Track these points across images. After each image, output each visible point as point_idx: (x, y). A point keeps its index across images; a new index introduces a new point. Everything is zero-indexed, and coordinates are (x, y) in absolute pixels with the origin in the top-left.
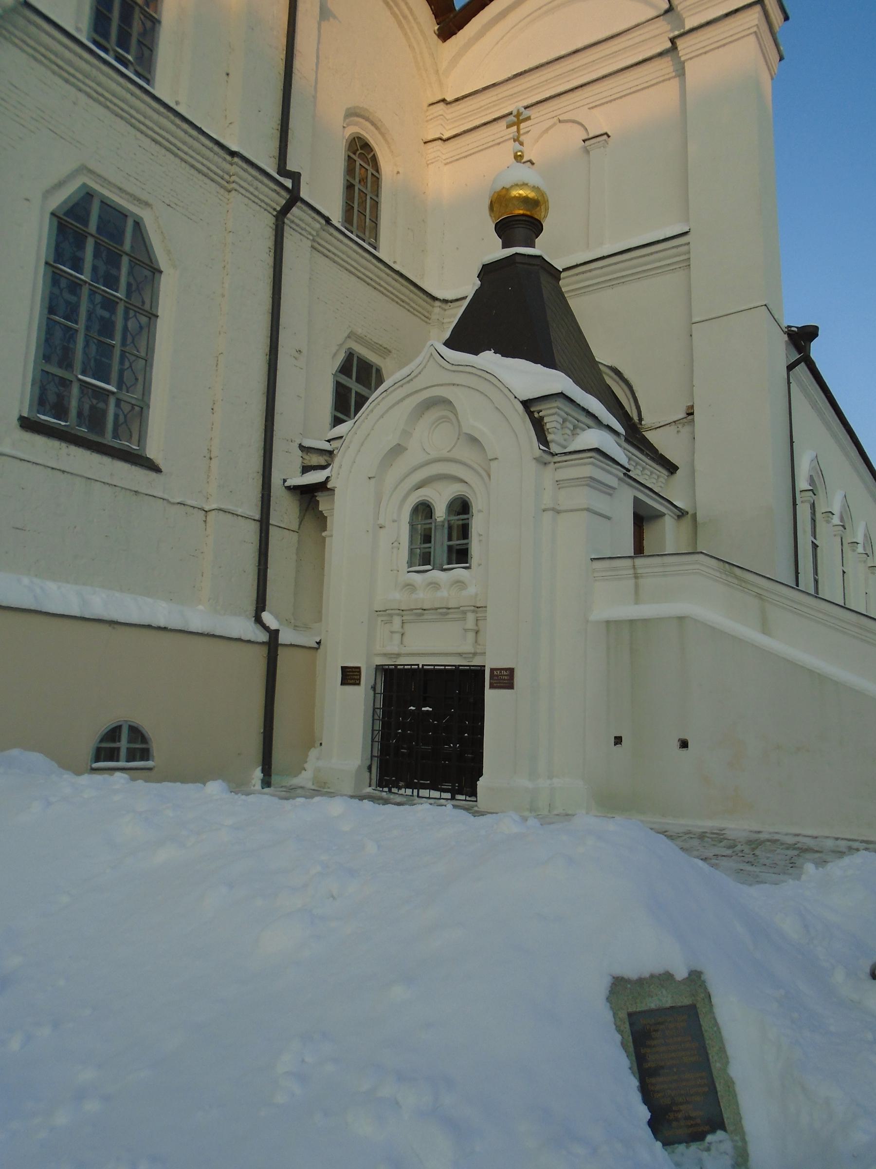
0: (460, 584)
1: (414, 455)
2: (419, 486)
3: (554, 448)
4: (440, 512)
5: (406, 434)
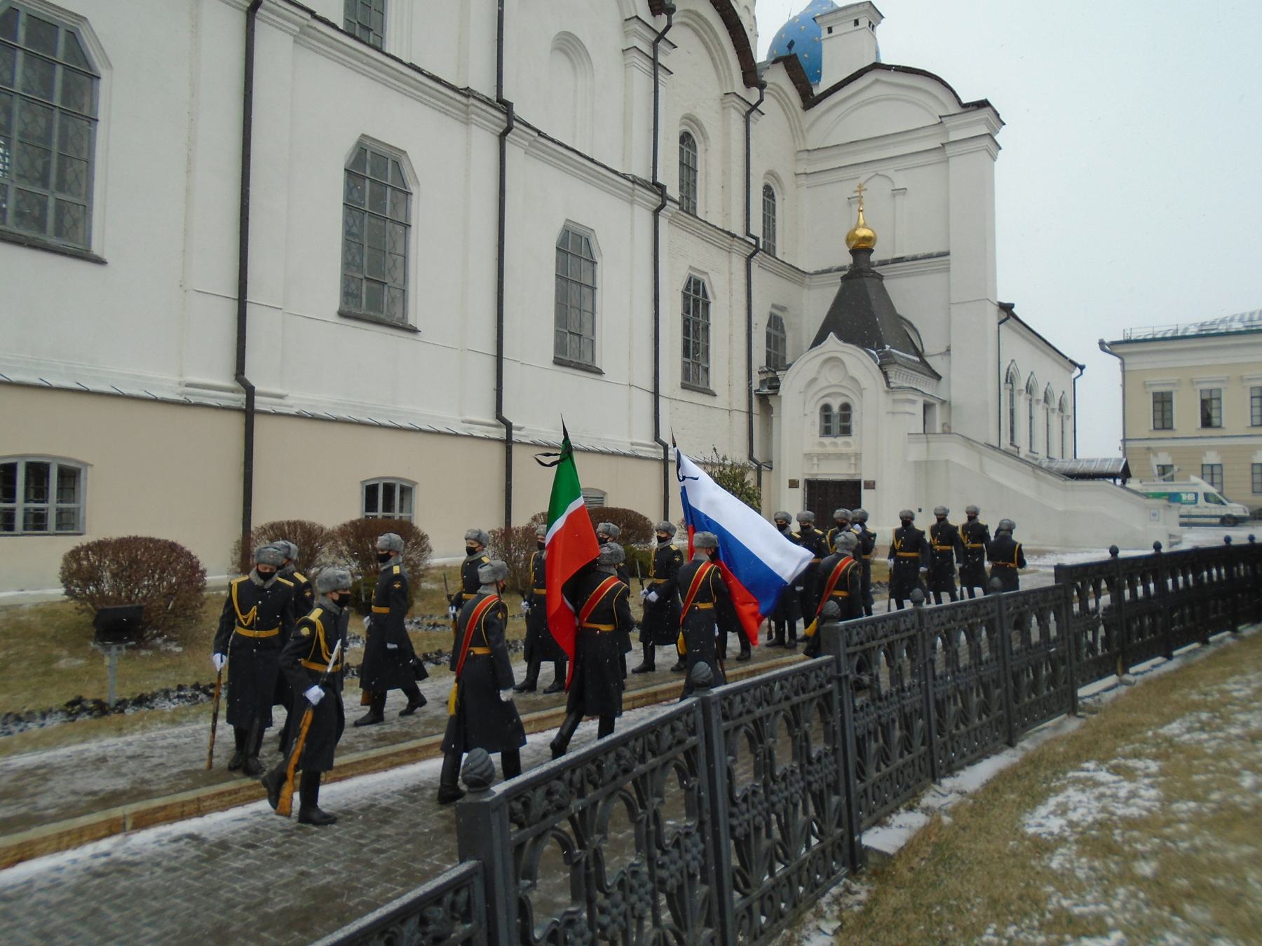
0: (848, 444)
1: (822, 383)
2: (825, 396)
3: (892, 385)
4: (836, 409)
5: (819, 373)
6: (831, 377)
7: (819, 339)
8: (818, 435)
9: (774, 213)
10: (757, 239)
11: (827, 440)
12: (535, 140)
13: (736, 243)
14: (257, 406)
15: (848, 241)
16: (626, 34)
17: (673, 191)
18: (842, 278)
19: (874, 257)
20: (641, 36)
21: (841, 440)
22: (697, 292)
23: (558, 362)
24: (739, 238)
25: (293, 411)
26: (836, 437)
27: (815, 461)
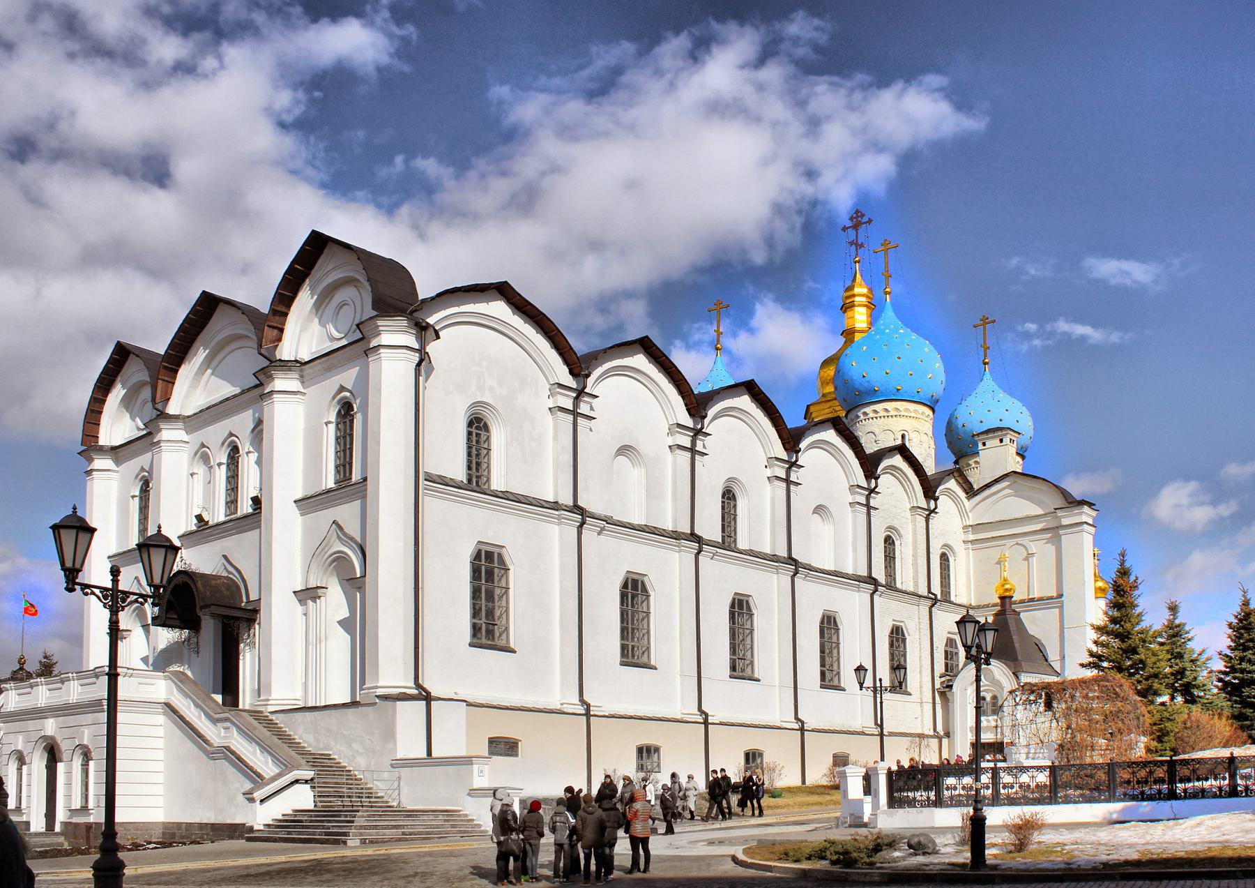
9: (949, 571)
12: (809, 573)
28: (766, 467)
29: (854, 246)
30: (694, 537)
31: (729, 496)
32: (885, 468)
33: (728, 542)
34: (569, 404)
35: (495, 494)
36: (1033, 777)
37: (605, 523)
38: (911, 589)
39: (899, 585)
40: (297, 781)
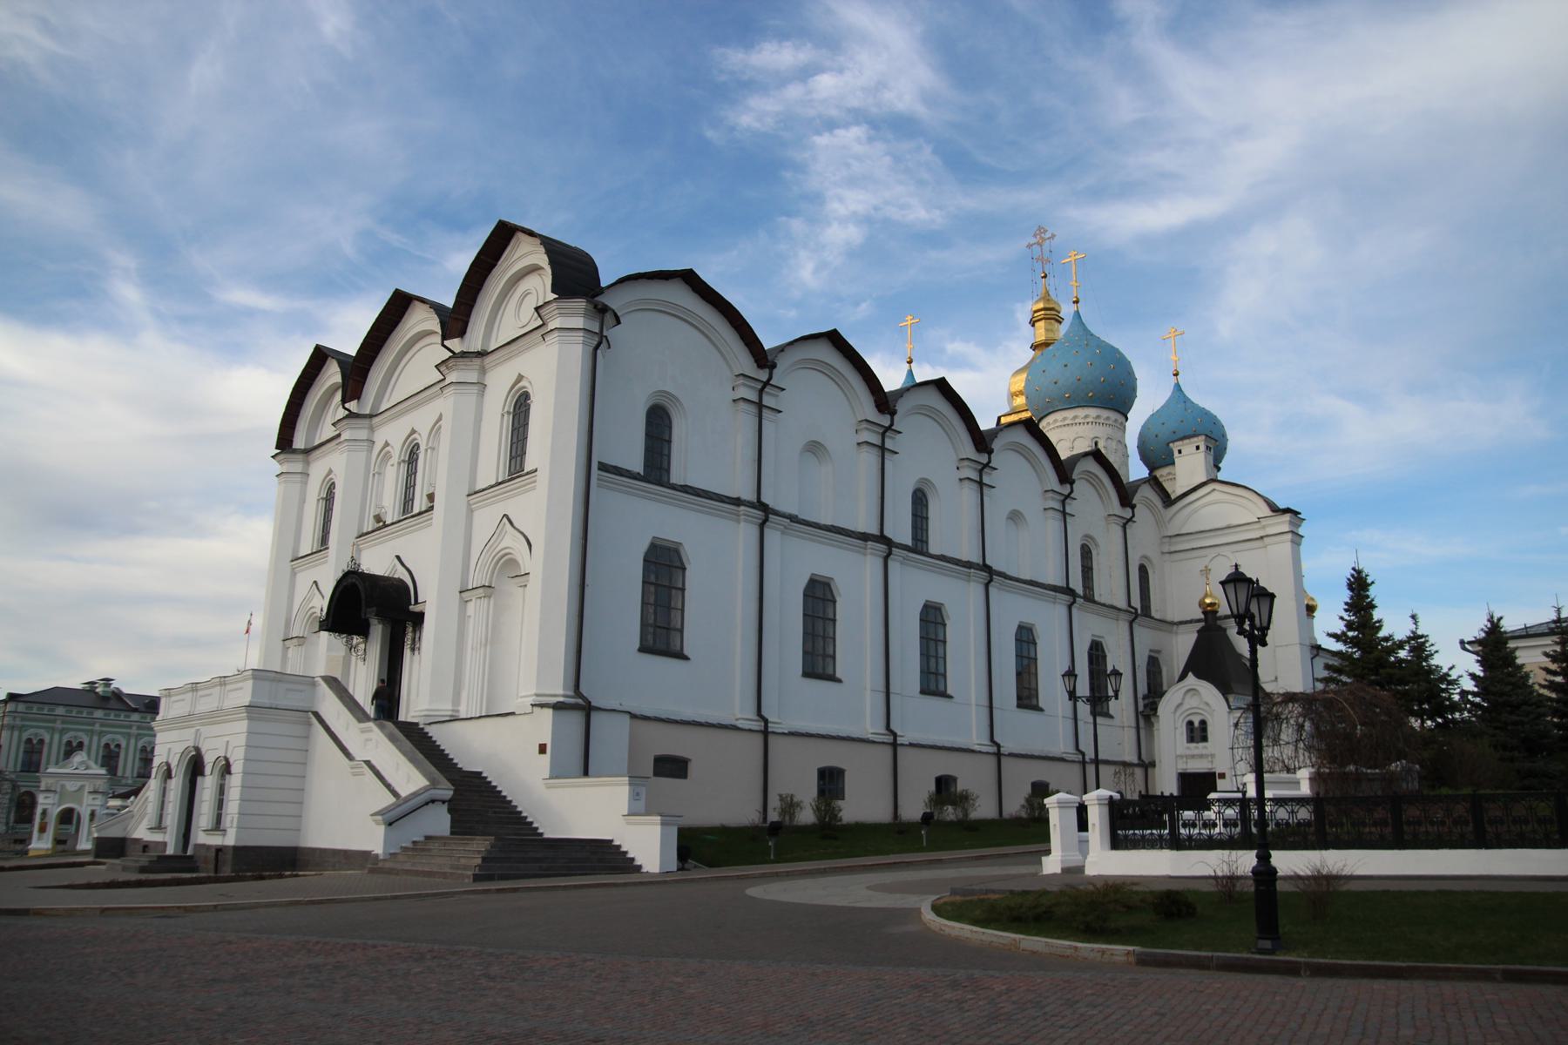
0: (1205, 747)
1: (1186, 706)
2: (1188, 715)
4: (1196, 724)
5: (1183, 699)
6: (1192, 702)
7: (1183, 677)
8: (1185, 741)
10: (1136, 609)
11: (1193, 745)
13: (1123, 616)
14: (898, 742)
15: (1200, 606)
16: (1046, 499)
17: (1079, 590)
18: (1198, 631)
19: (1219, 614)
20: (1053, 499)
21: (1201, 745)
22: (1097, 650)
23: (1019, 706)
24: (1124, 611)
25: (907, 743)
26: (1198, 742)
27: (1185, 759)
28: (958, 468)
29: (1045, 258)
30: (882, 539)
31: (920, 500)
32: (1079, 474)
33: (919, 544)
34: (753, 396)
35: (674, 487)
36: (1292, 812)
37: (788, 521)
38: (1109, 602)
39: (1096, 598)
40: (433, 801)
